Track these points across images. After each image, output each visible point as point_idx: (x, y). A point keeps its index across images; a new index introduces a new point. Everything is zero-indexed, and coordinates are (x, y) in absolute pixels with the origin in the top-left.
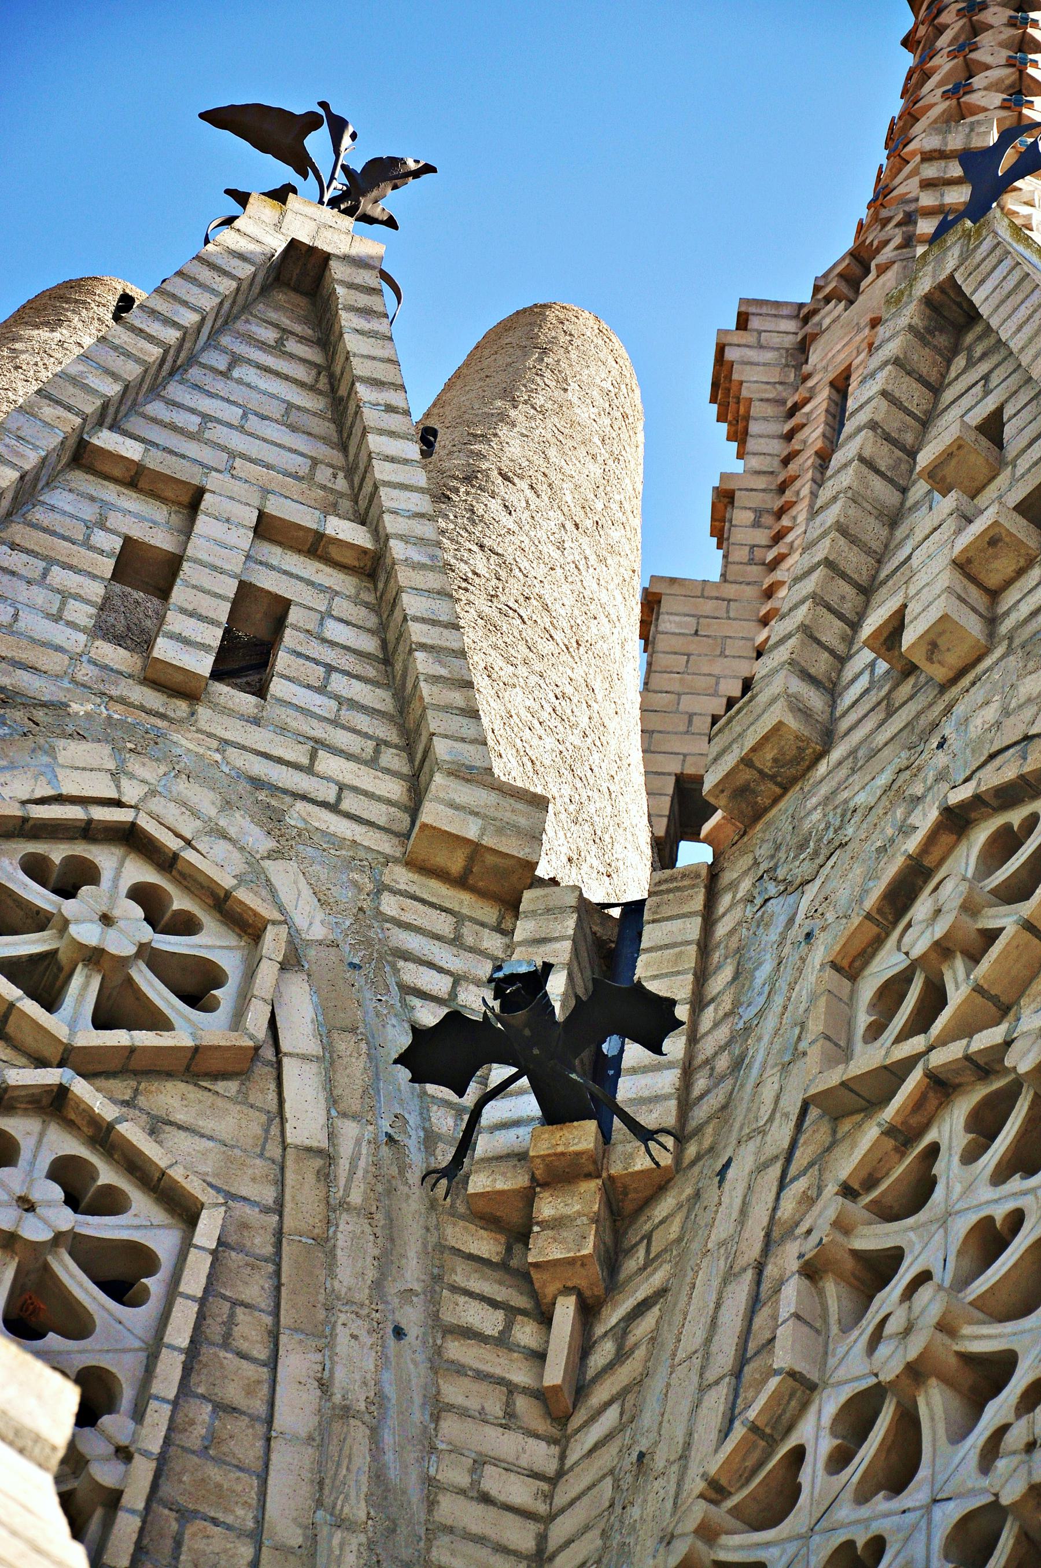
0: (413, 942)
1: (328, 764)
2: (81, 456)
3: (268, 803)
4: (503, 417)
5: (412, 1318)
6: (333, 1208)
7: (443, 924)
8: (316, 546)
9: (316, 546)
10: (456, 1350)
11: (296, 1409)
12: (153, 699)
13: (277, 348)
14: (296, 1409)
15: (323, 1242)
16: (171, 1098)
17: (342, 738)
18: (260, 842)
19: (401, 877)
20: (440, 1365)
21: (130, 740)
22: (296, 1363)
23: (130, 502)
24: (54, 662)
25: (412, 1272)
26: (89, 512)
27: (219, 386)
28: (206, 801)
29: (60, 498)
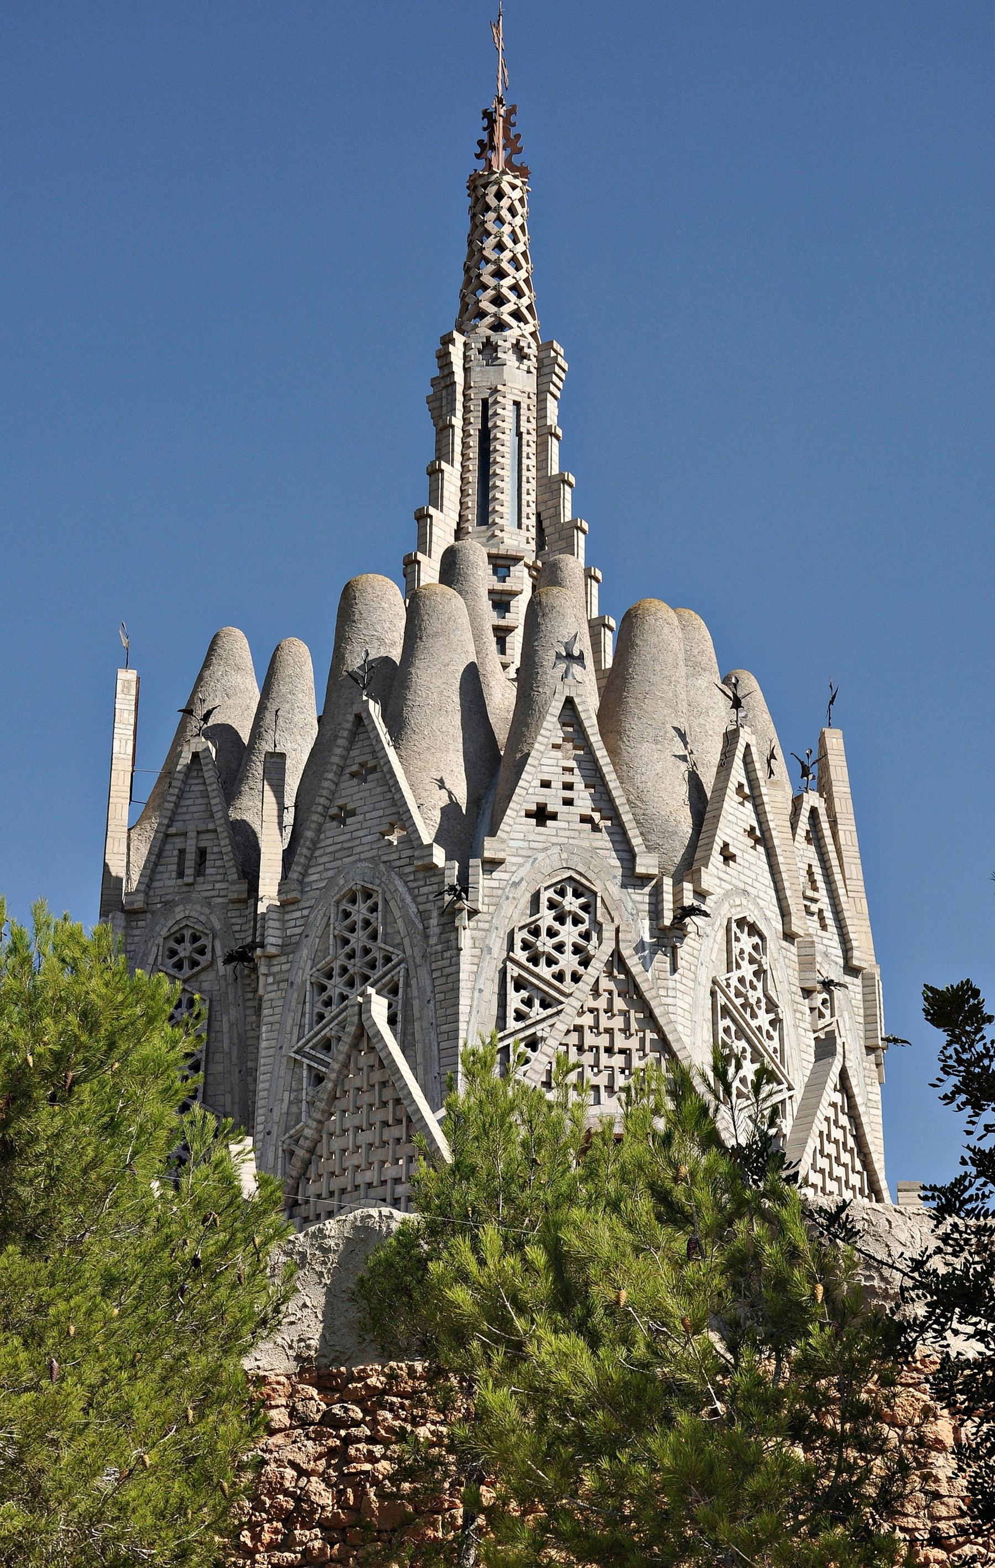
0: (234, 921)
1: (218, 886)
2: (167, 836)
3: (207, 902)
5: (240, 1002)
7: (237, 913)
8: (208, 831)
9: (208, 831)
10: (248, 1004)
11: (225, 1029)
12: (185, 889)
14: (225, 1029)
15: (227, 993)
16: (203, 977)
18: (207, 911)
19: (231, 906)
20: (246, 1008)
21: (186, 901)
22: (225, 1019)
27: (188, 795)
28: (198, 907)
29: (168, 847)
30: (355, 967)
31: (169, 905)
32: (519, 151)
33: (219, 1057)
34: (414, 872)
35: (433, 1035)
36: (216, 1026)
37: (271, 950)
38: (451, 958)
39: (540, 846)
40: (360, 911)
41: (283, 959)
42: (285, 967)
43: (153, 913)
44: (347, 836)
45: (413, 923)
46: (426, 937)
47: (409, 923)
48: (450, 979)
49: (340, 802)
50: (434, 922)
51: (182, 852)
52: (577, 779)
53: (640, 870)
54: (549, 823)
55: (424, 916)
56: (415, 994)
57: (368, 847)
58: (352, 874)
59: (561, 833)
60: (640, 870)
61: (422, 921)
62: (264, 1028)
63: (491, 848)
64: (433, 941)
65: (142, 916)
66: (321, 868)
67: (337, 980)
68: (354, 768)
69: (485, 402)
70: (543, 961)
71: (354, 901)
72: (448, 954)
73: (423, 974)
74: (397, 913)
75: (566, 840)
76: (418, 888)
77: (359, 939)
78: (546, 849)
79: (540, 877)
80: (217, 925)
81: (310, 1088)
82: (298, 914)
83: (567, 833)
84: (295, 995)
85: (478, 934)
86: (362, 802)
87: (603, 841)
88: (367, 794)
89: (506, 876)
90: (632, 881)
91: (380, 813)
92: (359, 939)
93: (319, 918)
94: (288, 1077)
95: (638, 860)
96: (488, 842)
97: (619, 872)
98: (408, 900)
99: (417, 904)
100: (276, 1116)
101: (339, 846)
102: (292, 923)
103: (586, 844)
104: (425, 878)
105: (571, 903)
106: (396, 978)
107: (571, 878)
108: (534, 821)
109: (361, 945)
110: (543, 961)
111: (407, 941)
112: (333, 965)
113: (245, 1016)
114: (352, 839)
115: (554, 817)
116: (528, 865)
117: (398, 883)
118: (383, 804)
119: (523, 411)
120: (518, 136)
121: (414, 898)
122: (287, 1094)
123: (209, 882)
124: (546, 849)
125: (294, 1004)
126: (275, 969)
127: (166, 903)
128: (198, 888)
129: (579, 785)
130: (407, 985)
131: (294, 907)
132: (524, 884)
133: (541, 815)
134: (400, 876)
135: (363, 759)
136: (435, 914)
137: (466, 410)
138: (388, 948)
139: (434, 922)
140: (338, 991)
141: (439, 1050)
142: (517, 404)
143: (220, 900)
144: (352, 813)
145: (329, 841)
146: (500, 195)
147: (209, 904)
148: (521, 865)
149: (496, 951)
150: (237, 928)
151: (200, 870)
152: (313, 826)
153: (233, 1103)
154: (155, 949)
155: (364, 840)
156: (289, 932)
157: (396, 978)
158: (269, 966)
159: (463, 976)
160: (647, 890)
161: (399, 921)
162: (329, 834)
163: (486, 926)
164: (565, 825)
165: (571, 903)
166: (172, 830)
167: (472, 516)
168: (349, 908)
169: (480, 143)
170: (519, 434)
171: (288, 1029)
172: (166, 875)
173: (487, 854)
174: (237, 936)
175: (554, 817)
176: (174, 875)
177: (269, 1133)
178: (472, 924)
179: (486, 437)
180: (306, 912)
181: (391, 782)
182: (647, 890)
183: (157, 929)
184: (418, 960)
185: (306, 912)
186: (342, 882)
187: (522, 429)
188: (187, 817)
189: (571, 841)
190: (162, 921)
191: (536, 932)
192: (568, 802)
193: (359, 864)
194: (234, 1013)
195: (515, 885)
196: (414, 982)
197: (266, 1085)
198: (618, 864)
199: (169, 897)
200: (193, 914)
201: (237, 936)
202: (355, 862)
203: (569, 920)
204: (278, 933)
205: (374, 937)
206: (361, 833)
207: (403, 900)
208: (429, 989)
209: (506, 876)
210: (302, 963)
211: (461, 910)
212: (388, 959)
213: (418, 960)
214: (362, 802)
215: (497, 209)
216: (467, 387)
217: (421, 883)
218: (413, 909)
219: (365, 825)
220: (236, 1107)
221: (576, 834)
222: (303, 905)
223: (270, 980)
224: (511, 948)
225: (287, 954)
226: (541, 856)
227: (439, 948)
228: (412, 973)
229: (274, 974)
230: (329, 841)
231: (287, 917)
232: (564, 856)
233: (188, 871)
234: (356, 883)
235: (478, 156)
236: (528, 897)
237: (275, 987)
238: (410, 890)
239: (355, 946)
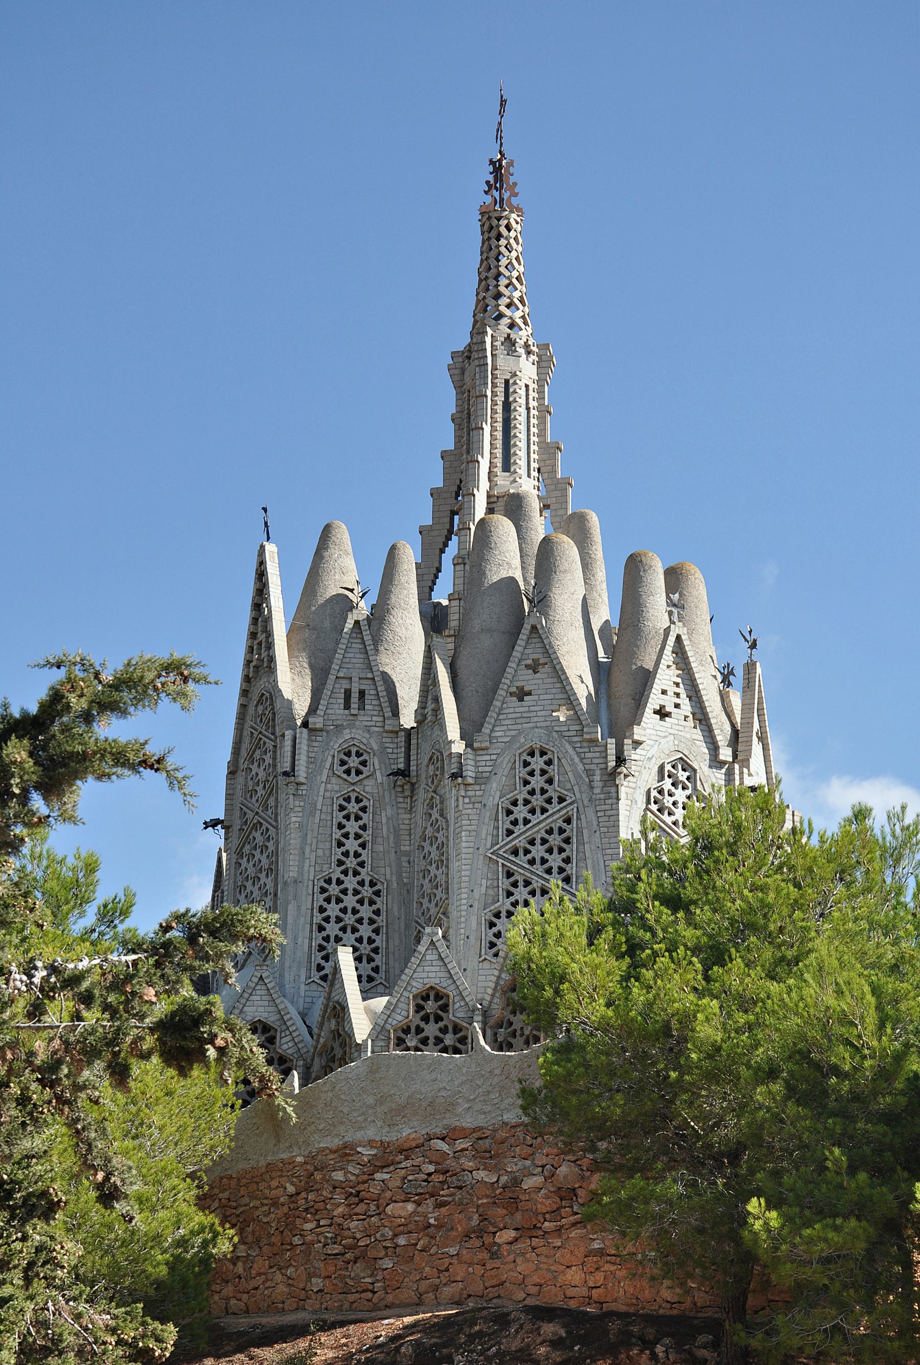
0: (387, 745)
1: (374, 718)
3: (367, 729)
4: (391, 591)
5: (394, 803)
6: (384, 790)
7: (390, 740)
8: (367, 678)
9: (367, 678)
10: (399, 805)
11: (384, 821)
12: (352, 718)
13: (356, 638)
14: (384, 821)
16: (365, 782)
17: (375, 713)
18: (368, 736)
19: (385, 734)
20: (398, 808)
21: (351, 726)
23: (344, 681)
24: (339, 717)
25: (393, 797)
26: (339, 686)
27: (351, 650)
28: (360, 732)
30: (538, 801)
31: (339, 728)
32: (516, 195)
33: (380, 840)
34: (580, 742)
35: (599, 855)
36: (377, 818)
37: (470, 781)
38: (612, 805)
39: (663, 734)
40: (538, 763)
41: (477, 787)
42: (478, 793)
43: (327, 732)
44: (526, 709)
45: (581, 777)
46: (592, 788)
47: (578, 776)
48: (612, 819)
49: (519, 684)
50: (597, 778)
51: (348, 694)
52: (681, 690)
53: (722, 757)
54: (667, 719)
55: (589, 773)
56: (584, 825)
57: (543, 719)
58: (530, 736)
59: (674, 727)
60: (722, 757)
61: (588, 776)
62: (463, 833)
63: (638, 732)
64: (597, 791)
65: (319, 733)
66: (505, 728)
67: (520, 807)
68: (529, 662)
69: (507, 382)
70: (666, 812)
71: (532, 754)
72: (609, 801)
73: (590, 813)
74: (568, 769)
75: (676, 732)
76: (585, 753)
77: (537, 782)
78: (666, 737)
79: (663, 755)
80: (375, 747)
81: (505, 880)
82: (488, 758)
83: (678, 727)
84: (488, 814)
85: (630, 791)
86: (537, 687)
87: (698, 734)
88: (540, 681)
89: (644, 753)
90: (714, 764)
91: (552, 697)
92: (537, 782)
93: (505, 763)
94: (485, 869)
95: (721, 751)
96: (636, 729)
97: (707, 757)
98: (577, 760)
99: (584, 764)
100: (476, 895)
101: (519, 715)
102: (483, 763)
103: (688, 736)
104: (589, 747)
105: (683, 776)
106: (570, 813)
107: (681, 758)
108: (658, 717)
109: (539, 786)
110: (666, 812)
111: (576, 788)
112: (518, 797)
113: (398, 814)
114: (529, 712)
115: (668, 715)
116: (656, 746)
117: (568, 746)
118: (553, 691)
119: (531, 392)
120: (515, 184)
121: (581, 759)
122: (484, 881)
123: (368, 715)
124: (666, 737)
125: (487, 820)
126: (470, 793)
127: (337, 726)
128: (360, 718)
129: (683, 695)
130: (578, 819)
131: (485, 752)
132: (654, 759)
133: (662, 713)
134: (570, 743)
135: (536, 656)
136: (598, 772)
137: (494, 385)
138: (563, 791)
139: (597, 778)
140: (522, 815)
141: (605, 866)
142: (527, 386)
143: (377, 729)
144: (529, 693)
145: (512, 710)
146: (508, 228)
147: (369, 731)
148: (652, 746)
149: (639, 802)
150: (390, 750)
151: (362, 707)
152: (501, 698)
153: (392, 874)
154: (330, 758)
155: (539, 713)
156: (480, 769)
157: (570, 813)
158: (466, 791)
159: (621, 818)
160: (723, 771)
161: (570, 774)
162: (510, 705)
163: (634, 785)
164: (676, 721)
165: (683, 776)
166: (341, 674)
167: (499, 462)
168: (529, 759)
169: (488, 182)
170: (528, 409)
171: (484, 836)
172: (336, 706)
173: (636, 737)
174: (390, 756)
175: (668, 715)
176: (342, 706)
177: (471, 906)
178: (625, 783)
179: (507, 406)
180: (494, 757)
181: (563, 677)
182: (723, 771)
183: (331, 744)
184: (586, 803)
185: (494, 757)
186: (522, 740)
187: (531, 406)
188: (350, 666)
189: (680, 733)
190: (335, 739)
191: (661, 792)
192: (677, 706)
193: (536, 730)
194: (389, 811)
195: (650, 759)
196: (583, 817)
197: (468, 873)
198: (707, 751)
199: (339, 722)
200: (357, 736)
201: (390, 756)
202: (533, 728)
203: (680, 786)
204: (473, 769)
205: (550, 781)
206: (536, 708)
207: (572, 760)
208: (595, 823)
209: (644, 753)
210: (492, 793)
211: (620, 773)
212: (561, 800)
213: (586, 803)
214: (537, 687)
215: (507, 238)
216: (494, 368)
217: (587, 750)
218: (580, 767)
219: (539, 703)
220: (394, 877)
221: (681, 728)
222: (490, 751)
223: (467, 800)
224: (648, 802)
225: (481, 784)
226: (663, 741)
227: (602, 796)
228: (581, 810)
229: (470, 797)
230: (512, 710)
231: (479, 758)
232: (676, 742)
233: (353, 706)
234: (537, 744)
235: (486, 193)
236: (656, 769)
237: (471, 806)
238: (578, 754)
239: (535, 786)
